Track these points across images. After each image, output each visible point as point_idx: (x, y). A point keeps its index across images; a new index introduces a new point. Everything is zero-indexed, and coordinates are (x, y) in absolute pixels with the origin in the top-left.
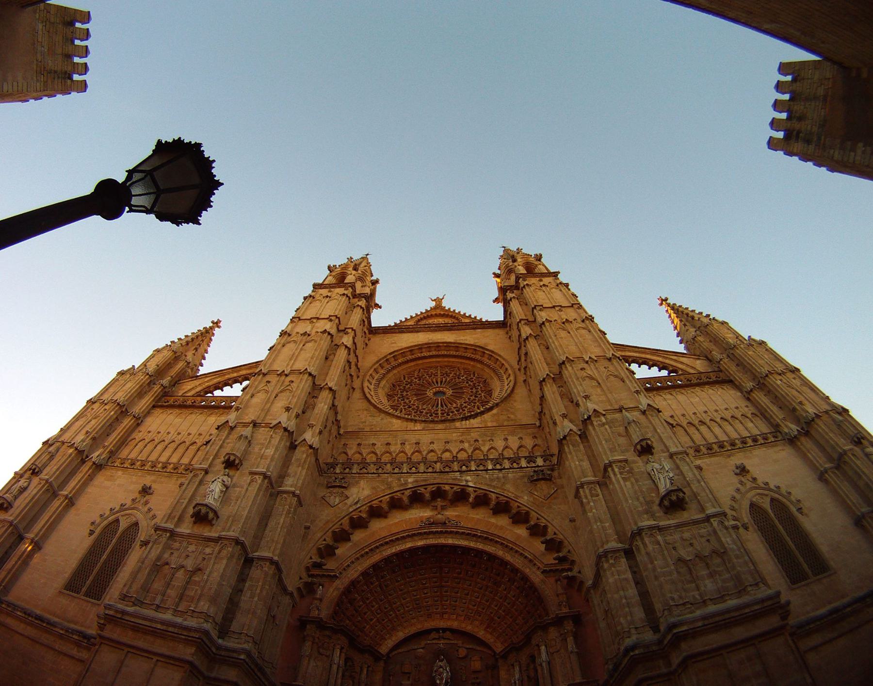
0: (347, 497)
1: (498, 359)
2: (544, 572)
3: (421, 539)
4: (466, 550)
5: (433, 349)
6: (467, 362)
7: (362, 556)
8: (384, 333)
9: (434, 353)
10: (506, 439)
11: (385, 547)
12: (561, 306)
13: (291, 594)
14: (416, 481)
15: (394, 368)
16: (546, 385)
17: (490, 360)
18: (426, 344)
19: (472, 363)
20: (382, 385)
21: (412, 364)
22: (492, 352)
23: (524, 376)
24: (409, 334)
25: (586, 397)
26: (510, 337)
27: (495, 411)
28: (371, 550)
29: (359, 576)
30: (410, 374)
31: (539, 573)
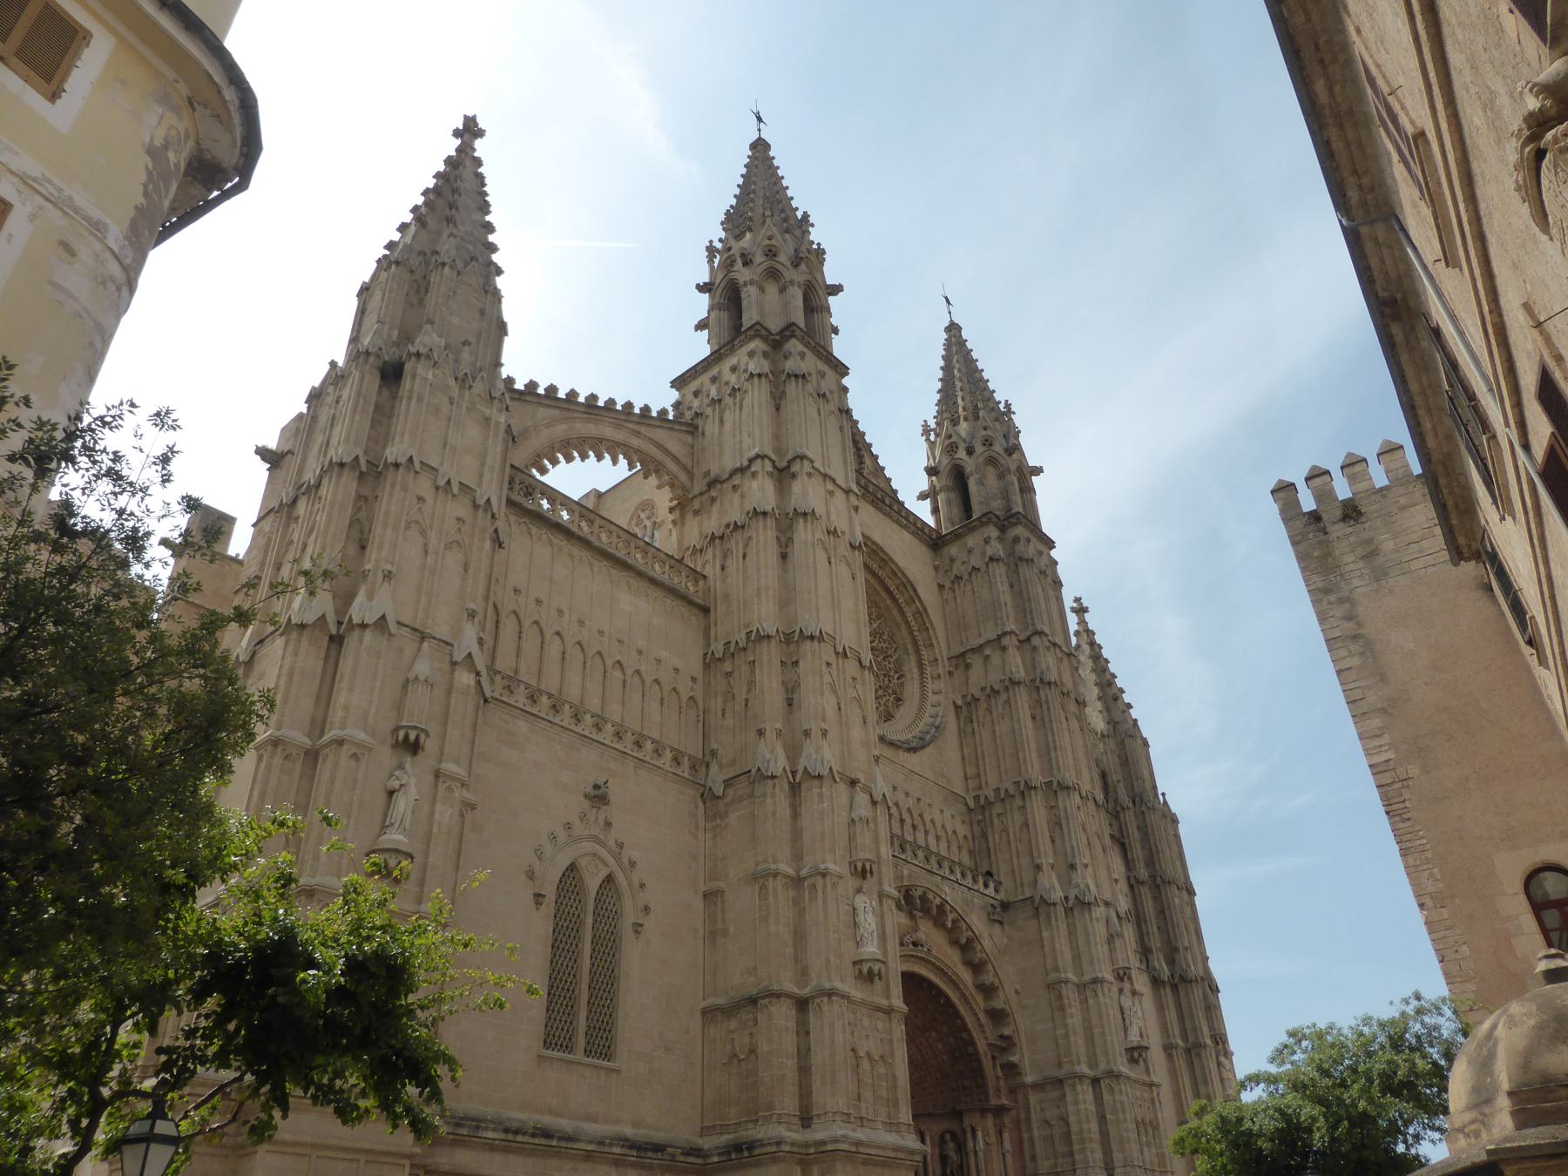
1: (927, 629)
2: (990, 1045)
4: (931, 985)
6: (884, 595)
10: (942, 811)
12: (1060, 647)
14: (909, 876)
16: (1036, 793)
17: (915, 618)
19: (888, 602)
22: (925, 610)
23: (960, 697)
25: (1086, 866)
26: (941, 587)
27: (929, 749)
31: (984, 1042)
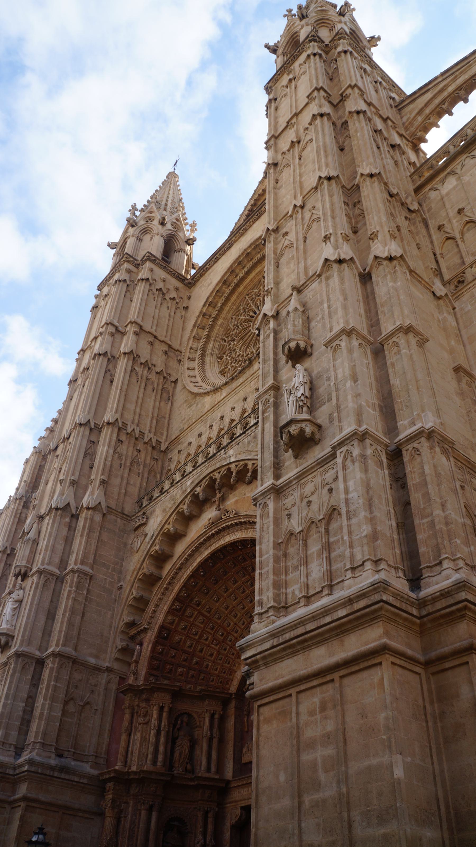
0: (146, 535)
3: (206, 549)
5: (246, 261)
7: (163, 594)
8: (201, 276)
9: (248, 266)
11: (181, 573)
13: (109, 670)
15: (216, 319)
18: (234, 263)
20: (209, 350)
21: (234, 297)
24: (223, 257)
28: (169, 583)
29: (166, 616)
30: (237, 313)
